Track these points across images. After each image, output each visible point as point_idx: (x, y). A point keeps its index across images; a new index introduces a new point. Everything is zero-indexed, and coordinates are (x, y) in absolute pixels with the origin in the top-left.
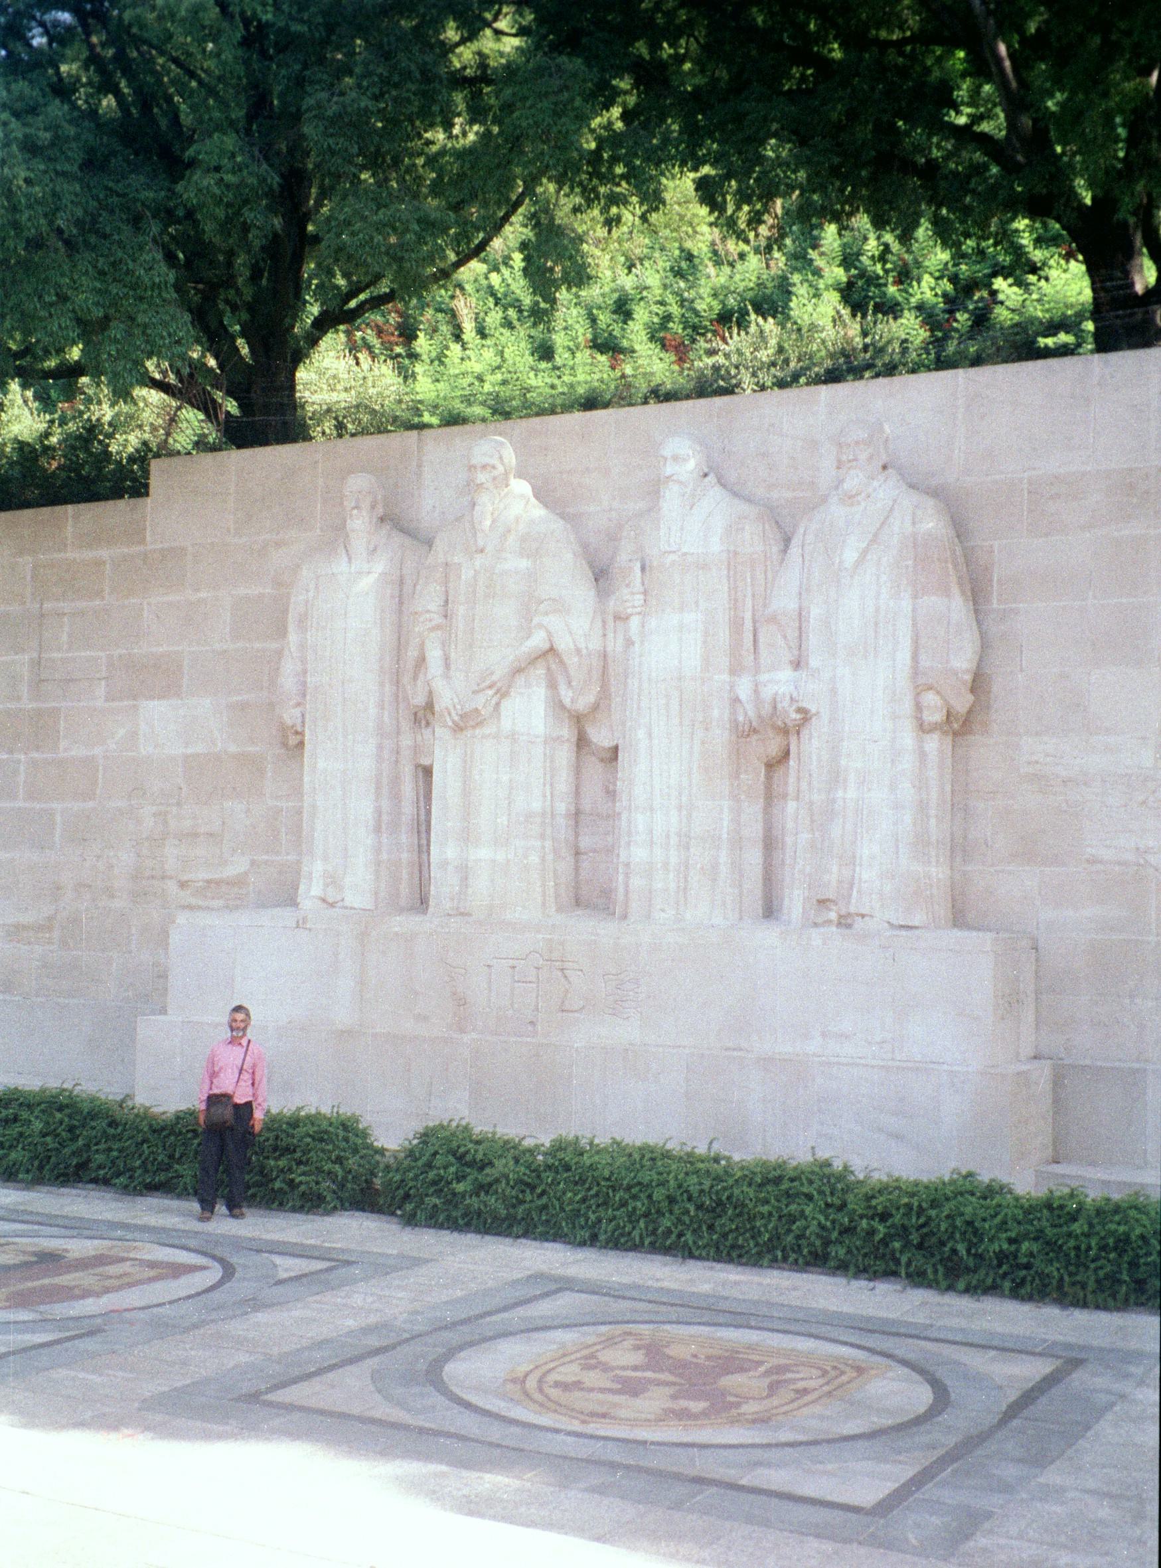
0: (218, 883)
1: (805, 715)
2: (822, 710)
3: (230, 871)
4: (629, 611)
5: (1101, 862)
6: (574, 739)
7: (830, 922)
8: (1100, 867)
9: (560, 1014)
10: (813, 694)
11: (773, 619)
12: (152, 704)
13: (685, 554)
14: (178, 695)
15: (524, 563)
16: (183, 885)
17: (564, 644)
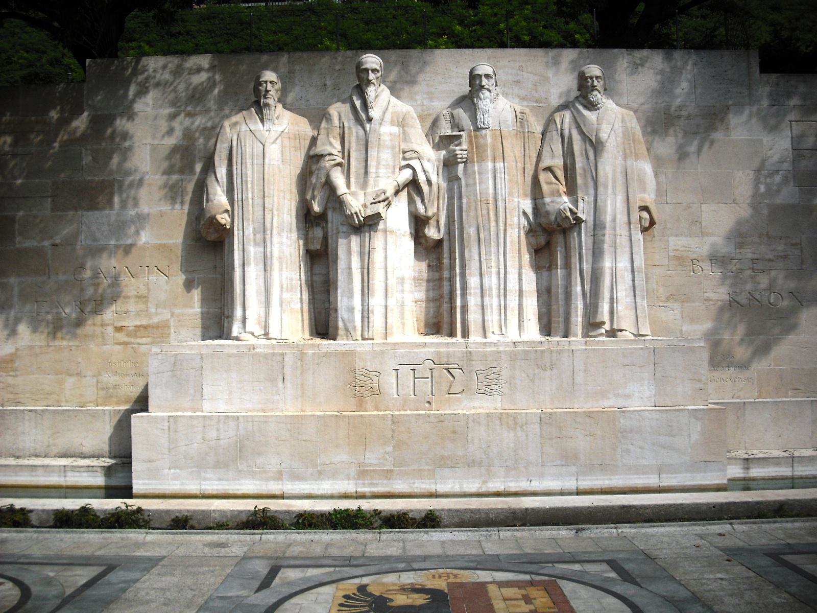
0: (145, 327)
1: (579, 221)
2: (588, 219)
3: (156, 320)
4: (459, 160)
7: (602, 334)
8: (711, 303)
9: (447, 396)
10: (584, 212)
11: (549, 169)
12: (90, 213)
15: (395, 129)
16: (119, 329)
17: (422, 178)
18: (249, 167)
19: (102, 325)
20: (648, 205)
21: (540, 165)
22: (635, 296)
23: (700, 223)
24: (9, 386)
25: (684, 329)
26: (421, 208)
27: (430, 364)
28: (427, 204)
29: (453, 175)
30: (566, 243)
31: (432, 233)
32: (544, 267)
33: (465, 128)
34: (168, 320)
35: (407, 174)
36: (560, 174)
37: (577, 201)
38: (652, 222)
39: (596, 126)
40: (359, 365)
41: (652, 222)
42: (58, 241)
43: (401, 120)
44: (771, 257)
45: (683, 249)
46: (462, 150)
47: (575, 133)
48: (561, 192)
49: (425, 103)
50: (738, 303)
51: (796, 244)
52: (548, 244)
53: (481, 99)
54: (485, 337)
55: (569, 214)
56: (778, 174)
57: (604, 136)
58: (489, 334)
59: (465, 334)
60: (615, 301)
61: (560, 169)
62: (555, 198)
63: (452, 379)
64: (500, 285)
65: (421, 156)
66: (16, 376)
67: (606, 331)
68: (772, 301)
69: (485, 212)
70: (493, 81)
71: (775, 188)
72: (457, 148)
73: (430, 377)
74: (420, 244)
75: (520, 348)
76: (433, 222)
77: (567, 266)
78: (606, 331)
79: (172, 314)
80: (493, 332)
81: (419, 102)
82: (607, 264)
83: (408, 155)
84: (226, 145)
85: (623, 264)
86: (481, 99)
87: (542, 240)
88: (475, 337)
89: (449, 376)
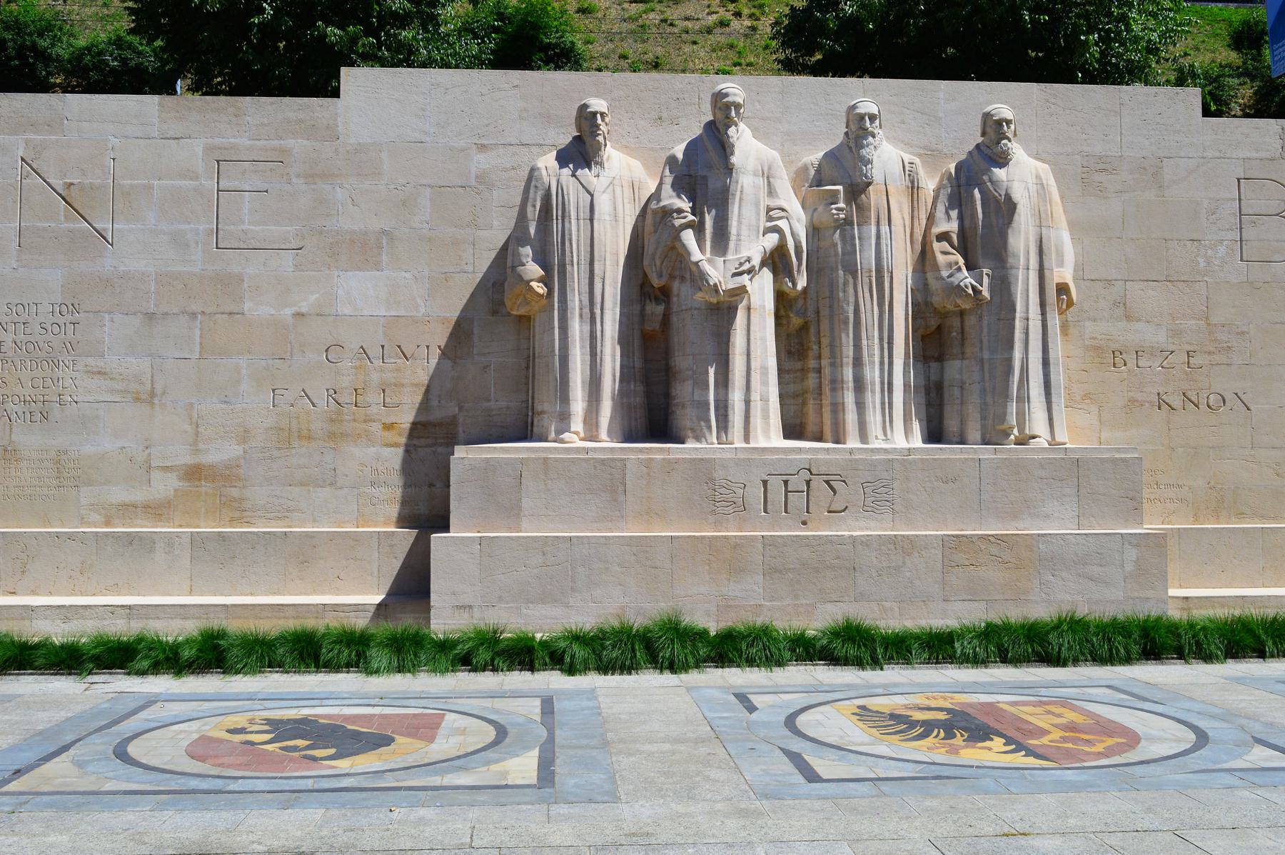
11: (943, 237)
14: (377, 266)
18: (574, 222)
19: (365, 421)
24: (235, 500)
27: (807, 475)
34: (454, 417)
35: (772, 240)
40: (719, 474)
42: (304, 310)
43: (766, 169)
51: (1243, 333)
55: (970, 291)
58: (871, 438)
66: (244, 487)
79: (461, 408)
84: (540, 193)
87: (933, 323)
88: (853, 443)
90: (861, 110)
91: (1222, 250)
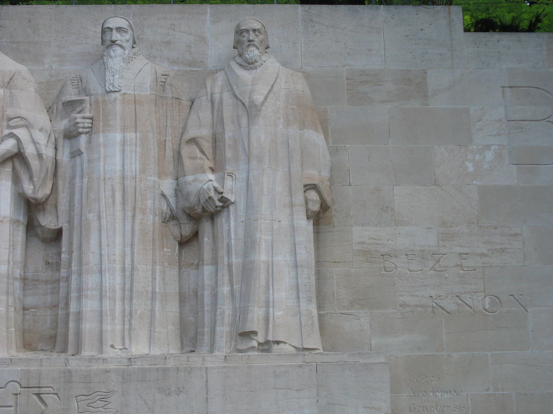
1: (225, 203)
4: (81, 130)
5: (408, 306)
6: (26, 223)
7: (253, 348)
8: (408, 309)
10: (232, 189)
11: (193, 141)
13: (125, 94)
17: (29, 150)
20: (316, 182)
21: (184, 137)
22: (298, 298)
23: (392, 209)
25: (374, 342)
26: (28, 189)
28: (35, 183)
29: (75, 149)
30: (213, 233)
31: (47, 221)
32: (193, 264)
33: (92, 92)
36: (207, 146)
37: (223, 178)
38: (325, 207)
39: (250, 87)
41: (325, 207)
43: (7, 80)
44: (485, 251)
45: (371, 241)
46: (84, 118)
47: (227, 96)
48: (206, 167)
49: (54, 67)
50: (443, 309)
51: (516, 235)
52: (196, 235)
53: (111, 57)
54: (102, 353)
56: (490, 150)
57: (259, 98)
58: (107, 348)
59: (78, 350)
60: (271, 304)
61: (208, 141)
62: (198, 175)
63: (43, 408)
64: (124, 285)
65: (30, 124)
67: (259, 344)
68: (487, 307)
69: (109, 193)
70: (128, 36)
71: (486, 166)
72: (79, 115)
73: (14, 405)
74: (37, 235)
75: (138, 365)
76: (49, 207)
77: (215, 262)
78: (259, 344)
80: (112, 346)
81: (47, 66)
82: (262, 257)
83: (12, 123)
85: (283, 258)
86: (111, 57)
89: (40, 403)
90: (106, 25)
91: (489, 155)
